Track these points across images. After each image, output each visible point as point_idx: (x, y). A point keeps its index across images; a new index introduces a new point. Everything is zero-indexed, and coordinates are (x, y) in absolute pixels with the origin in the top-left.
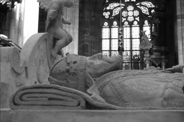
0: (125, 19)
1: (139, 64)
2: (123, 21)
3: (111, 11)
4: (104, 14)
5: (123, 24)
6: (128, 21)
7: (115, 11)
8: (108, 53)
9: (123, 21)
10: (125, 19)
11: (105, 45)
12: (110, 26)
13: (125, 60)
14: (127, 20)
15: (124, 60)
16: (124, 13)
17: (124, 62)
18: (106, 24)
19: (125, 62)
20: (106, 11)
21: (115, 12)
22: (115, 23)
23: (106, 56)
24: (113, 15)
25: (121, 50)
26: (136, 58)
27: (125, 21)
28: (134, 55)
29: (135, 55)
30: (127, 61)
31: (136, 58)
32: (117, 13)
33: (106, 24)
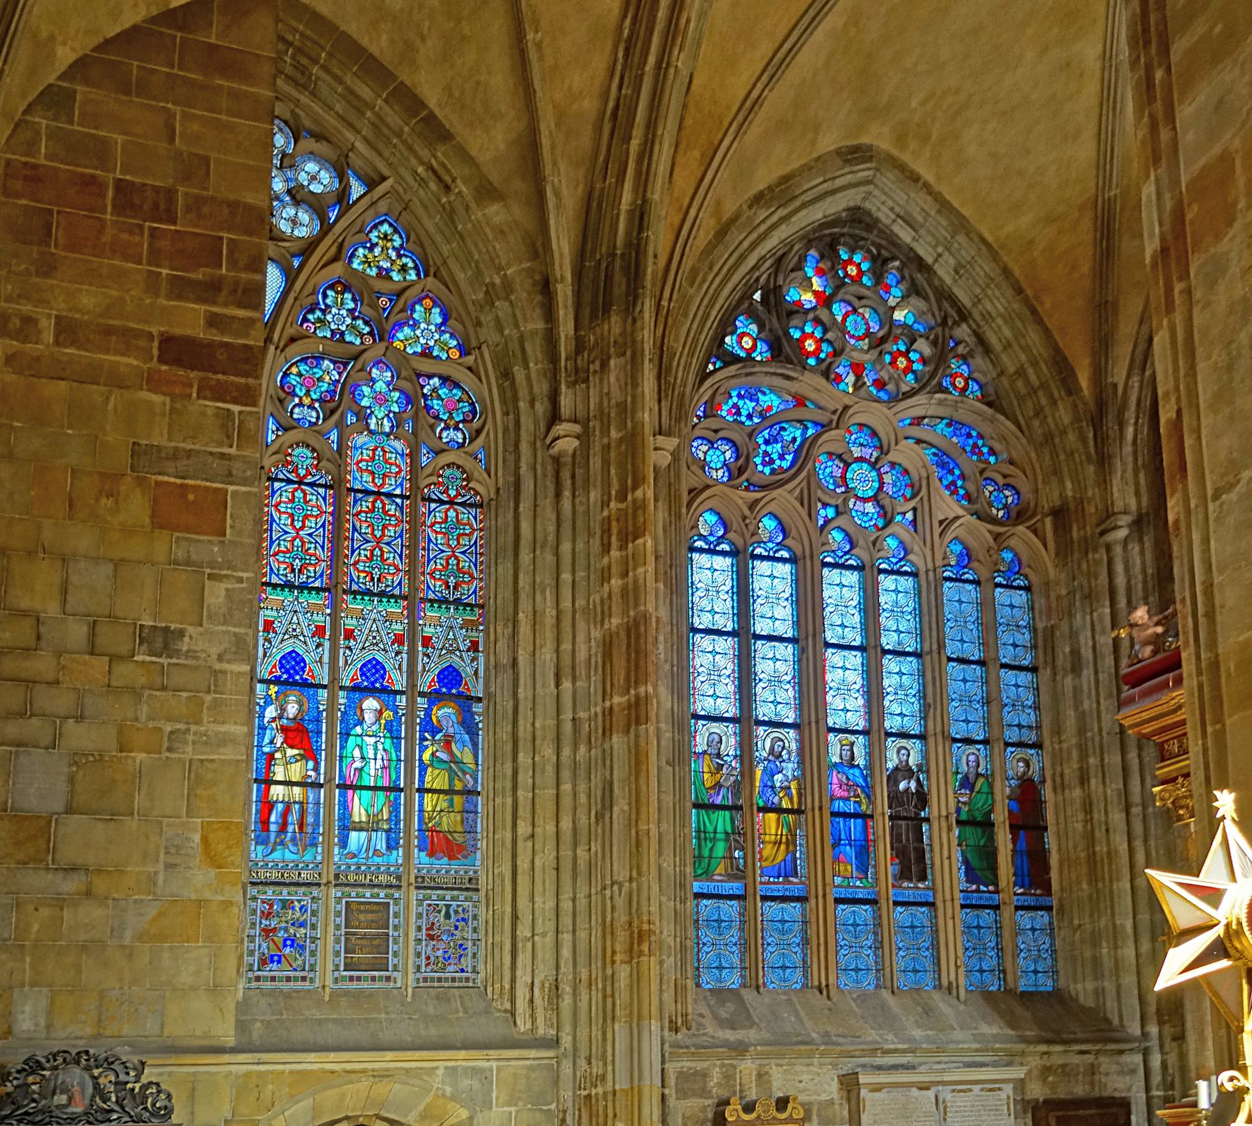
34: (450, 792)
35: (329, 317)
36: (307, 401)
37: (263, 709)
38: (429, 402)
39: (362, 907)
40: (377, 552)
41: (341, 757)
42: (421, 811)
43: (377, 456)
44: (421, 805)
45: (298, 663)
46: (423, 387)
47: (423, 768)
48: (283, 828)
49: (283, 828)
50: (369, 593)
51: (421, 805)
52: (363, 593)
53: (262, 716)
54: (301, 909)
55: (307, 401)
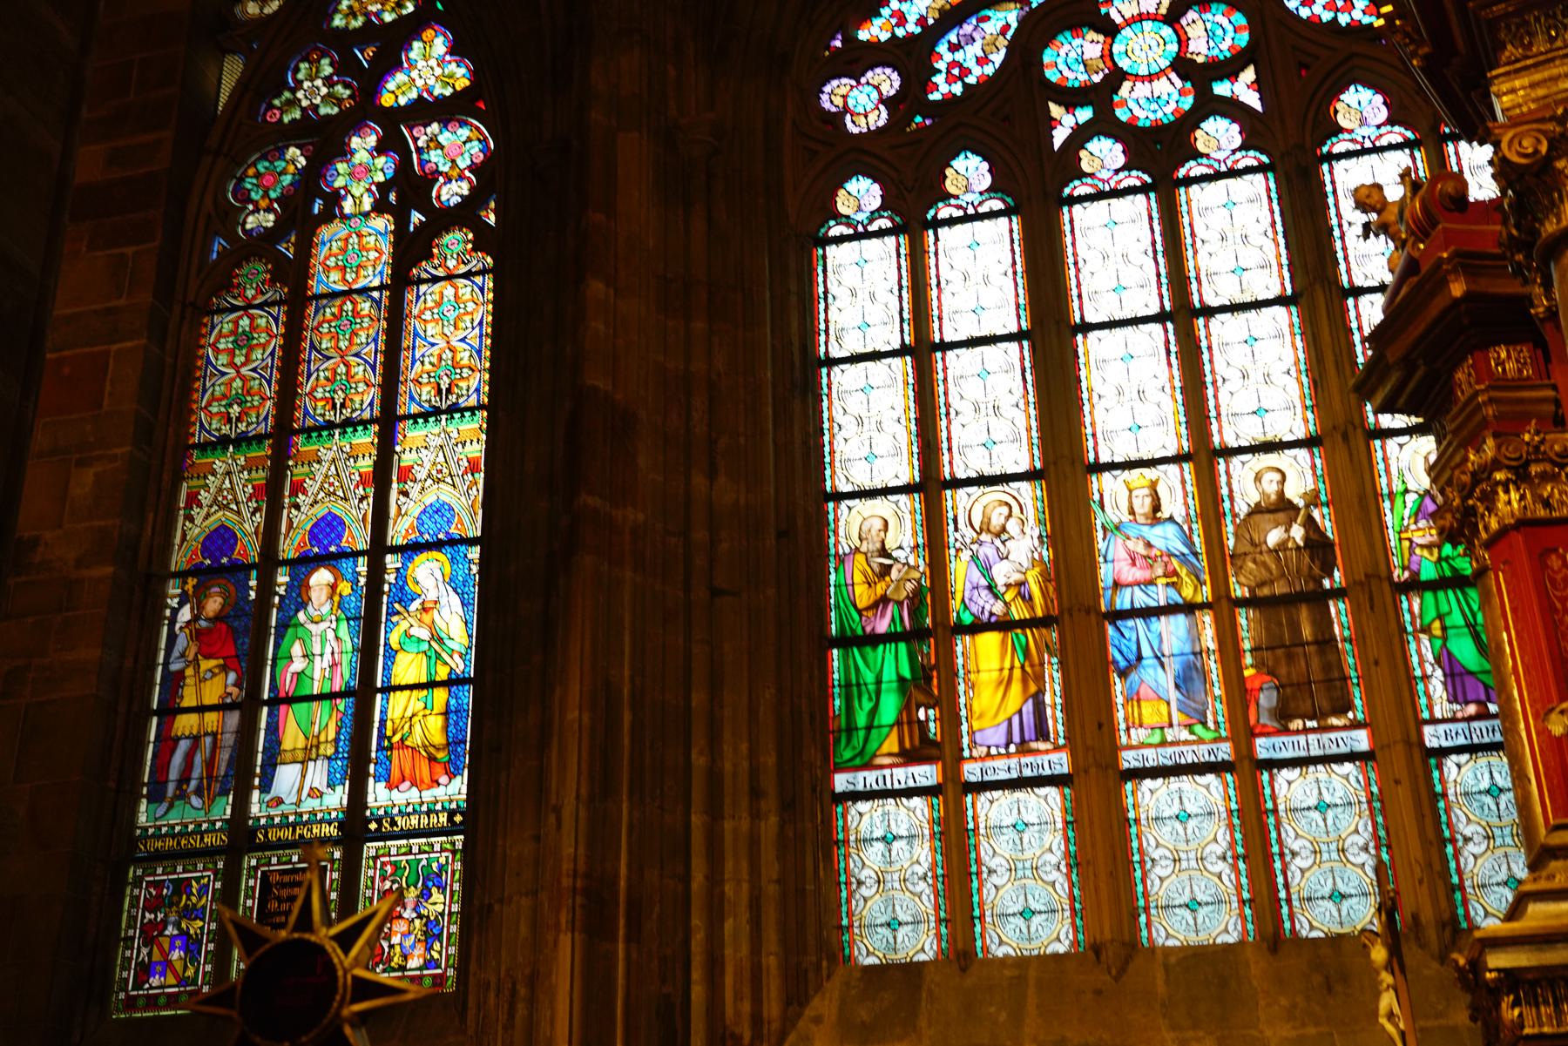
0: (1085, 114)
1: (1339, 611)
2: (1060, 136)
3: (912, 56)
4: (835, 92)
5: (1068, 163)
6: (1128, 134)
7: (954, 48)
8: (899, 525)
9: (1060, 136)
10: (1085, 114)
11: (865, 426)
12: (914, 213)
13: (1130, 574)
14: (1105, 124)
15: (1117, 585)
16: (1070, 58)
17: (1123, 601)
18: (861, 195)
19: (1141, 599)
20: (858, 60)
21: (959, 56)
22: (969, 173)
23: (884, 552)
24: (943, 88)
25: (1064, 459)
26: (1274, 537)
27: (1081, 136)
28: (1242, 509)
29: (1257, 510)
30: (1160, 595)
31: (1282, 546)
32: (982, 61)
33: (861, 195)
34: (431, 685)
35: (300, 95)
36: (263, 204)
37: (175, 612)
38: (425, 157)
39: (286, 879)
40: (342, 369)
41: (274, 660)
42: (383, 722)
43: (356, 248)
44: (384, 712)
45: (225, 541)
46: (415, 140)
47: (391, 655)
48: (185, 778)
49: (185, 778)
50: (330, 426)
51: (384, 712)
52: (319, 429)
53: (173, 621)
54: (199, 891)
55: (263, 204)
